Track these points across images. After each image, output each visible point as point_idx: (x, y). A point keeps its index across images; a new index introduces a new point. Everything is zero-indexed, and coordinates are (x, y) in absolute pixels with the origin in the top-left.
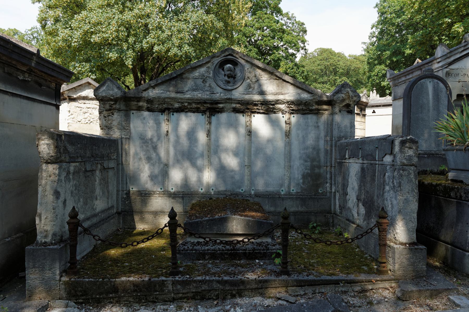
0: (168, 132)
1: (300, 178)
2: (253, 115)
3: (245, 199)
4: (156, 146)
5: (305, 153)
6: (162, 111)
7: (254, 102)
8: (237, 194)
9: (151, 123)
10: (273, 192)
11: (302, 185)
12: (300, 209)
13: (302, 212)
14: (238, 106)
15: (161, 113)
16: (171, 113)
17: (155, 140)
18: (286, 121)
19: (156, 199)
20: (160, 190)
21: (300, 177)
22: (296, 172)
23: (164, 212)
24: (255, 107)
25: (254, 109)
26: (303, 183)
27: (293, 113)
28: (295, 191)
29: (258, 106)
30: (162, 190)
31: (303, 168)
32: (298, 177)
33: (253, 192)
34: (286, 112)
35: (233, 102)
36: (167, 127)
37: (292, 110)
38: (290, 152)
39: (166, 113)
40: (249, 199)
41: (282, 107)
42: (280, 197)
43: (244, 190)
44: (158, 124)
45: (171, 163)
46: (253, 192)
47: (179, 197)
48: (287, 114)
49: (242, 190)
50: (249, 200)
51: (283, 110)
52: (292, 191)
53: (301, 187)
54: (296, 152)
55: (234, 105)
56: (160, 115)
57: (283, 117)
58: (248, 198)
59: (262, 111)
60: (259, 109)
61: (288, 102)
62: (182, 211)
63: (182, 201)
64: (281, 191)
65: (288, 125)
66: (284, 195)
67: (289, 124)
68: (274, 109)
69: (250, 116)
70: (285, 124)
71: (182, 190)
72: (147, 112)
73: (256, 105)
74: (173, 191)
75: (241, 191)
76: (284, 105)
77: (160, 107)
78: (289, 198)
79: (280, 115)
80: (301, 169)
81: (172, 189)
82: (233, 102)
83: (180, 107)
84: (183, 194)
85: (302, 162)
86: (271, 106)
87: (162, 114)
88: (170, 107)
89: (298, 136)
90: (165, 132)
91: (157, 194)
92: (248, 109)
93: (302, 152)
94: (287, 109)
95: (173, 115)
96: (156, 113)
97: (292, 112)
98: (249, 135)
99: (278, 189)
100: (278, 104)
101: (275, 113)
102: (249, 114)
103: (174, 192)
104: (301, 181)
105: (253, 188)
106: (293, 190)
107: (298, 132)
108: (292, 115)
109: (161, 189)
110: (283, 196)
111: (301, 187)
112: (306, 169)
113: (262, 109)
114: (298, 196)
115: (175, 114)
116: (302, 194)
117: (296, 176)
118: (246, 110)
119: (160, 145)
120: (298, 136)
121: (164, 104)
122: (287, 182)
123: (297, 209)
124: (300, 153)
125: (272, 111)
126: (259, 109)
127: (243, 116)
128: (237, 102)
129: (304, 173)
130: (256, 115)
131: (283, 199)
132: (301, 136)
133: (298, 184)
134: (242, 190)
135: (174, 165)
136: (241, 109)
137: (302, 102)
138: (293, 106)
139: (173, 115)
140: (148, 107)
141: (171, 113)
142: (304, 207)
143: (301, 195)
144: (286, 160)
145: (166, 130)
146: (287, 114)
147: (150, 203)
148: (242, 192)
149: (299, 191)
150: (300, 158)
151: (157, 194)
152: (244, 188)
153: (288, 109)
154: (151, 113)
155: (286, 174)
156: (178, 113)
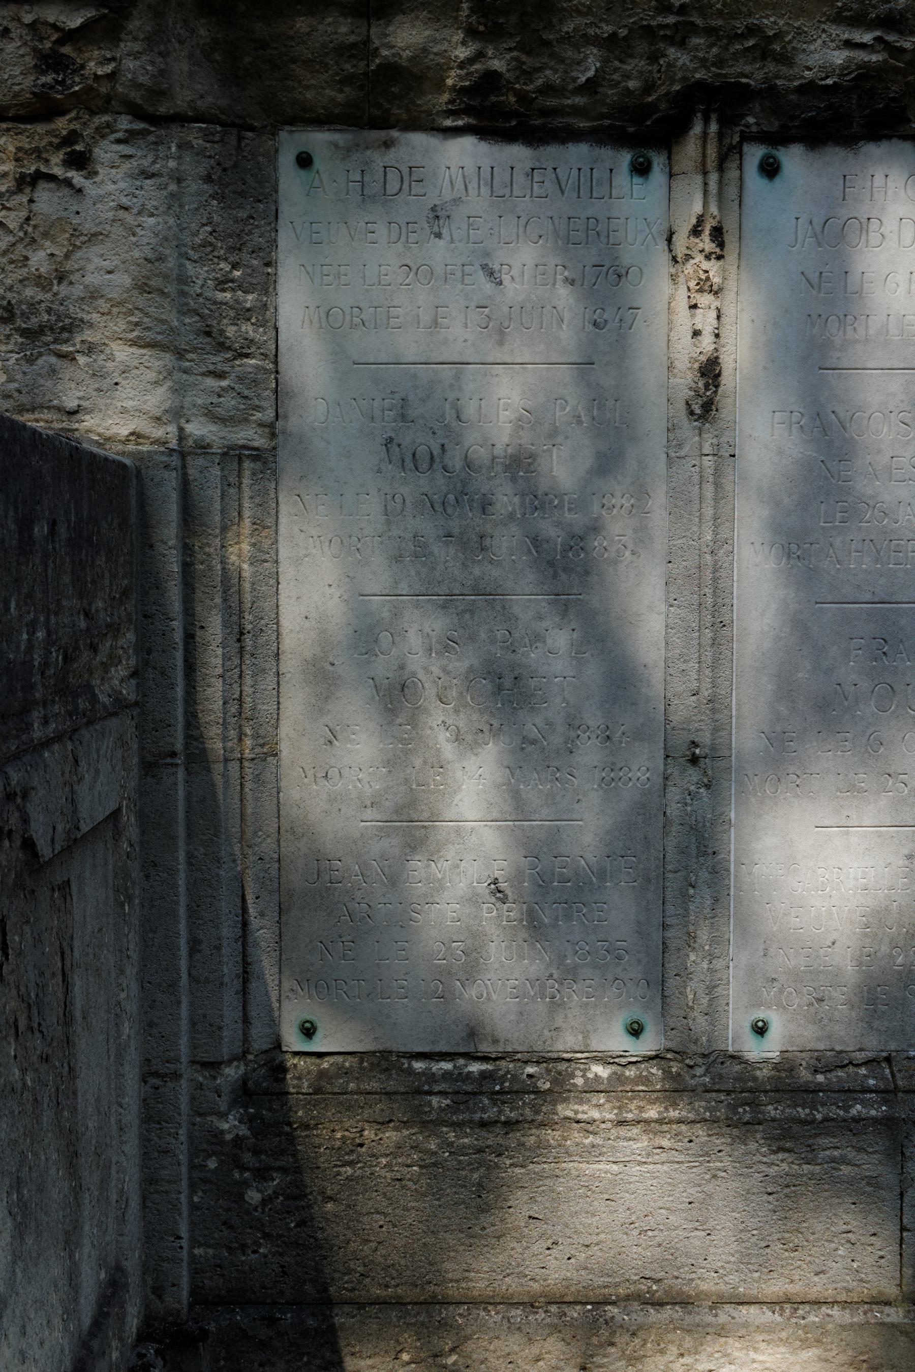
0: (710, 371)
4: (578, 542)
6: (646, 132)
9: (527, 264)
15: (625, 158)
16: (754, 154)
17: (562, 469)
19: (592, 1153)
20: (616, 1041)
23: (685, 1302)
30: (648, 1044)
36: (706, 320)
39: (690, 149)
44: (605, 283)
45: (746, 734)
47: (853, 1127)
56: (623, 178)
62: (892, 1291)
63: (889, 1176)
71: (873, 1045)
72: (468, 143)
74: (767, 1050)
77: (632, 74)
81: (768, 1026)
83: (863, 79)
84: (888, 1093)
87: (641, 169)
88: (752, 73)
90: (685, 380)
91: (593, 1088)
95: (770, 169)
96: (577, 154)
103: (785, 1066)
109: (635, 1031)
115: (793, 159)
119: (618, 529)
121: (679, 36)
135: (781, 751)
139: (770, 169)
140: (491, 79)
141: (754, 154)
145: (686, 354)
147: (521, 1205)
151: (593, 1088)
154: (518, 153)
156: (835, 155)
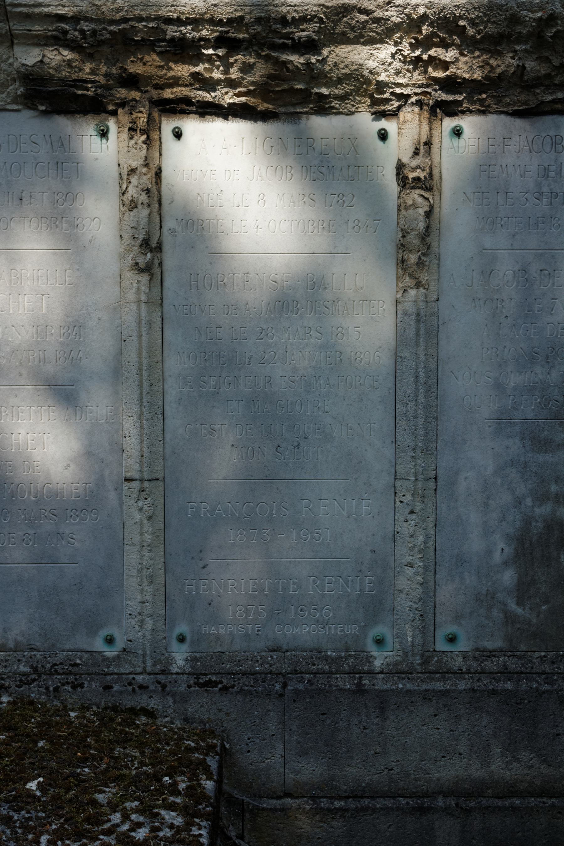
1: (497, 557)
2: (168, 126)
3: (129, 702)
5: (531, 389)
7: (172, 31)
8: (74, 672)
10: (318, 651)
11: (512, 606)
12: (500, 768)
13: (511, 790)
14: (57, 57)
18: (400, 167)
21: (501, 549)
22: (474, 517)
24: (183, 70)
25: (176, 82)
26: (522, 591)
27: (450, 109)
28: (463, 645)
29: (199, 58)
31: (522, 489)
32: (489, 552)
33: (180, 656)
34: (404, 98)
35: (18, 27)
37: (450, 84)
38: (430, 382)
40: (153, 704)
41: (379, 59)
42: (360, 690)
43: (120, 644)
46: (180, 656)
48: (410, 114)
49: (110, 641)
50: (151, 714)
51: (381, 86)
52: (441, 646)
53: (509, 618)
54: (473, 380)
55: (29, 57)
57: (383, 136)
58: (142, 700)
59: (228, 98)
60: (209, 85)
61: (413, 24)
64: (371, 648)
65: (415, 196)
66: (394, 671)
67: (427, 184)
68: (314, 75)
69: (149, 134)
70: (393, 187)
73: (185, 50)
75: (99, 645)
76: (385, 51)
78: (427, 696)
79: (364, 121)
80: (506, 498)
82: (18, 27)
85: (514, 446)
86: (297, 60)
89: (488, 273)
92: (132, 81)
93: (514, 380)
94: (409, 81)
97: (447, 100)
98: (147, 269)
99: (353, 630)
100: (344, 40)
101: (323, 107)
102: (142, 120)
104: (508, 577)
105: (183, 628)
106: (452, 639)
107: (488, 242)
108: (449, 123)
110: (381, 685)
111: (509, 618)
112: (542, 498)
113: (231, 84)
114: (486, 683)
116: (513, 665)
117: (475, 544)
118: (122, 93)
120: (488, 273)
122: (408, 583)
123: (477, 772)
124: (499, 386)
125: (305, 97)
126: (209, 85)
127: (104, 134)
128: (50, 28)
129: (528, 522)
130: (192, 126)
131: (383, 703)
132: (506, 267)
133: (486, 599)
134: (110, 641)
136: (81, 83)
137: (514, 20)
138: (449, 55)
142: (524, 755)
143: (506, 673)
144: (405, 438)
146: (410, 114)
148: (110, 652)
149: (489, 645)
150: (502, 422)
152: (128, 627)
153: (417, 77)
155: (405, 529)
